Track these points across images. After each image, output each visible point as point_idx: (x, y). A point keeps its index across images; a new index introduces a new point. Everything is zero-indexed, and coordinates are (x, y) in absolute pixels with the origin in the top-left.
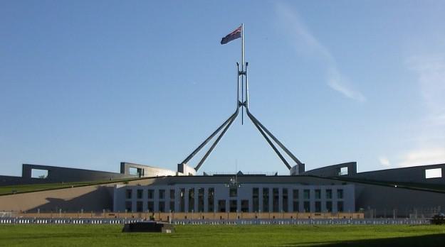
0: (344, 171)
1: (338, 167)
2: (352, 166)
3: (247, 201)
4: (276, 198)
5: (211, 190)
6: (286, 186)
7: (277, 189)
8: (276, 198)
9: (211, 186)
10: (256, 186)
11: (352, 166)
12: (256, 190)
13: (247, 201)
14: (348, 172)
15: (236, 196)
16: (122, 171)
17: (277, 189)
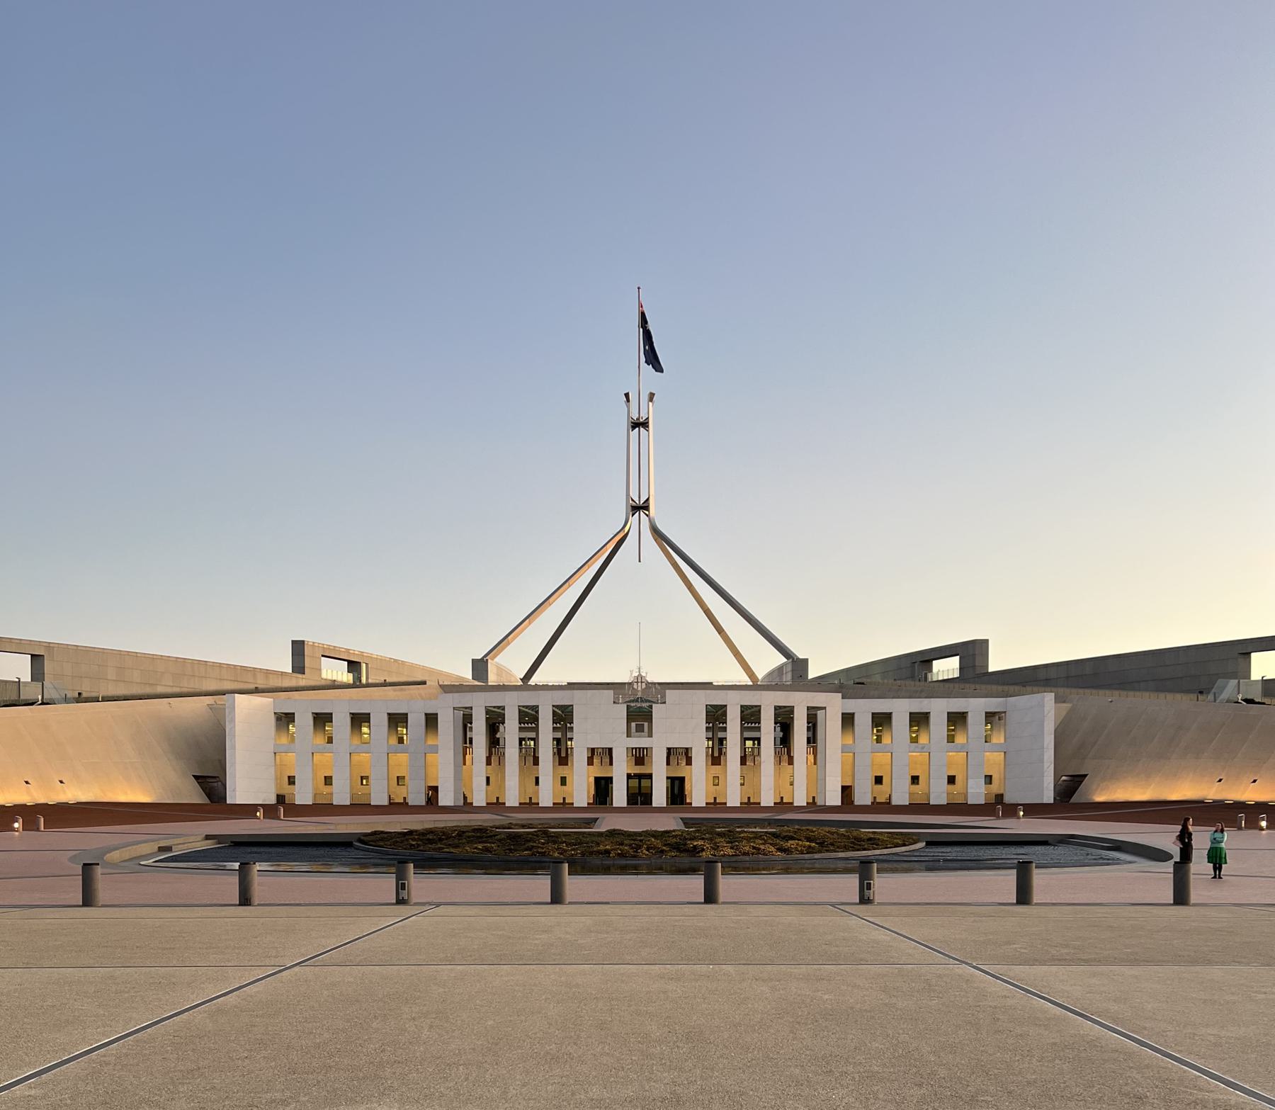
0: (946, 668)
1: (924, 659)
2: (972, 653)
3: (687, 750)
4: (785, 740)
5: (563, 717)
6: (817, 699)
7: (790, 710)
8: (785, 740)
9: (563, 699)
10: (717, 699)
11: (972, 653)
12: (716, 716)
13: (687, 750)
14: (962, 668)
15: (650, 735)
16: (299, 667)
17: (790, 710)
